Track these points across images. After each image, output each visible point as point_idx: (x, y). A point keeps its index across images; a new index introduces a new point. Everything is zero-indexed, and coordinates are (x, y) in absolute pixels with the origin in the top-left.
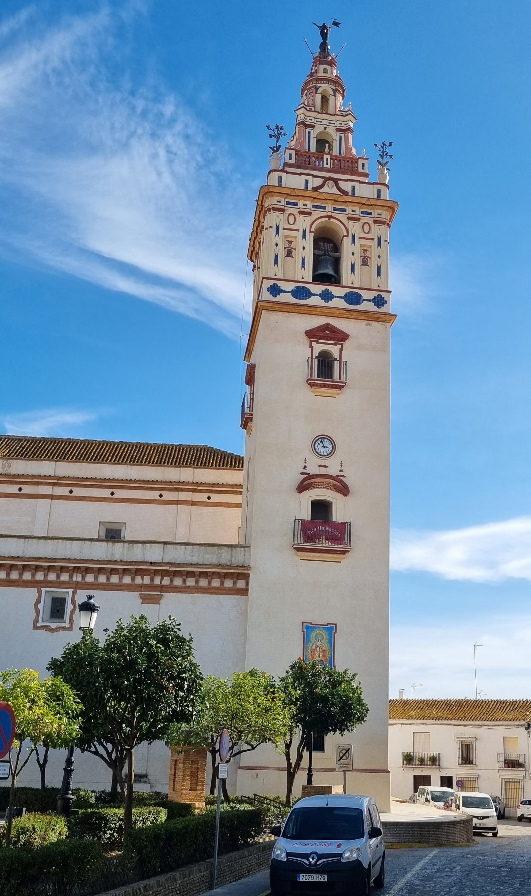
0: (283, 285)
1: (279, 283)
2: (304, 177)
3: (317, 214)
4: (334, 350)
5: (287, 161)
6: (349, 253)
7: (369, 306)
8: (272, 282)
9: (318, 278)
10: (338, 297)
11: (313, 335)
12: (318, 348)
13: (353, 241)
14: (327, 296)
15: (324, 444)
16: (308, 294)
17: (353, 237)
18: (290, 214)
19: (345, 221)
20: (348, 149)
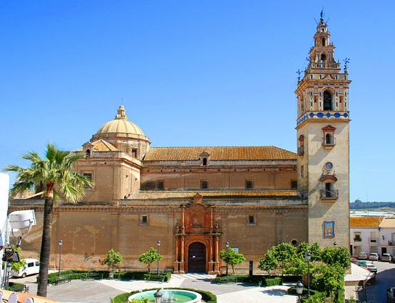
0: (314, 113)
3: (325, 87)
4: (331, 133)
6: (336, 99)
7: (342, 117)
9: (325, 109)
11: (324, 129)
12: (326, 133)
14: (328, 115)
15: (329, 165)
19: (333, 87)
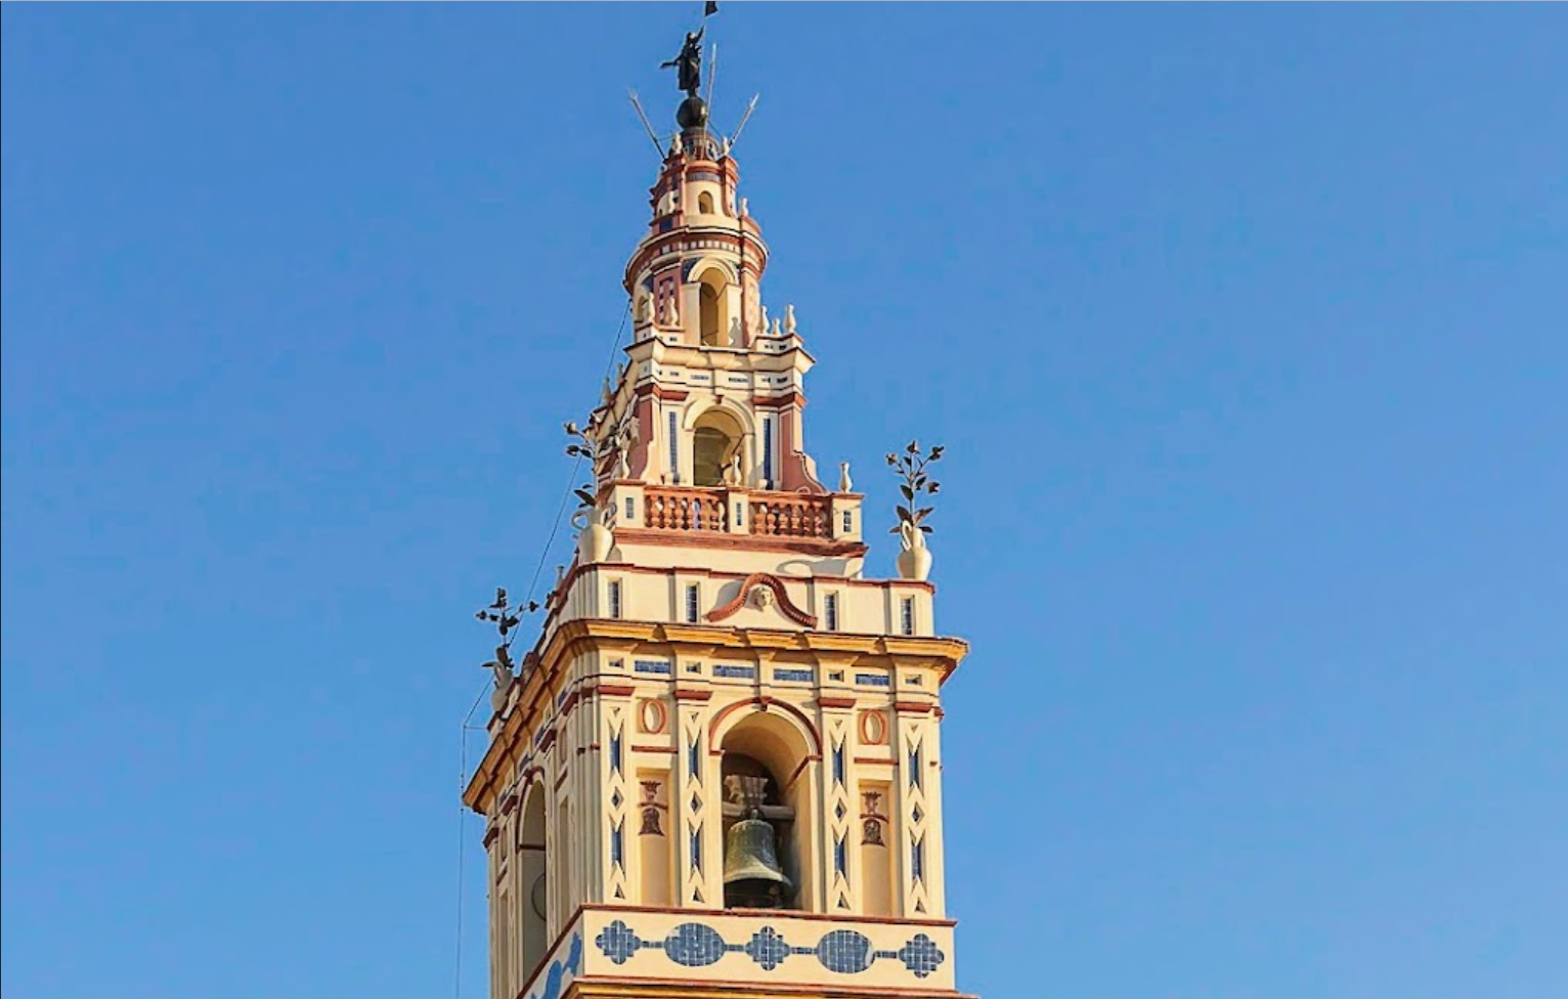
1: (630, 920)
2: (684, 582)
5: (621, 521)
6: (830, 809)
8: (607, 919)
9: (742, 895)
10: (800, 951)
13: (840, 773)
14: (767, 950)
16: (717, 947)
17: (839, 756)
18: (645, 700)
20: (792, 462)
